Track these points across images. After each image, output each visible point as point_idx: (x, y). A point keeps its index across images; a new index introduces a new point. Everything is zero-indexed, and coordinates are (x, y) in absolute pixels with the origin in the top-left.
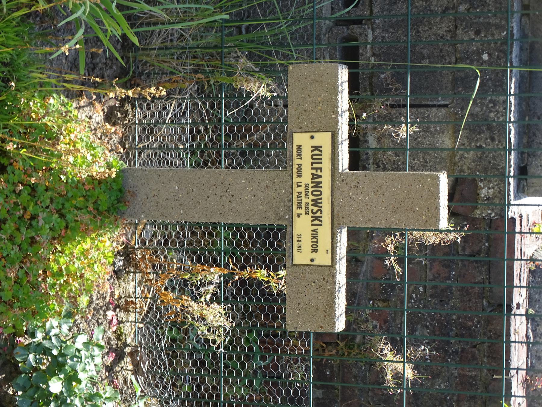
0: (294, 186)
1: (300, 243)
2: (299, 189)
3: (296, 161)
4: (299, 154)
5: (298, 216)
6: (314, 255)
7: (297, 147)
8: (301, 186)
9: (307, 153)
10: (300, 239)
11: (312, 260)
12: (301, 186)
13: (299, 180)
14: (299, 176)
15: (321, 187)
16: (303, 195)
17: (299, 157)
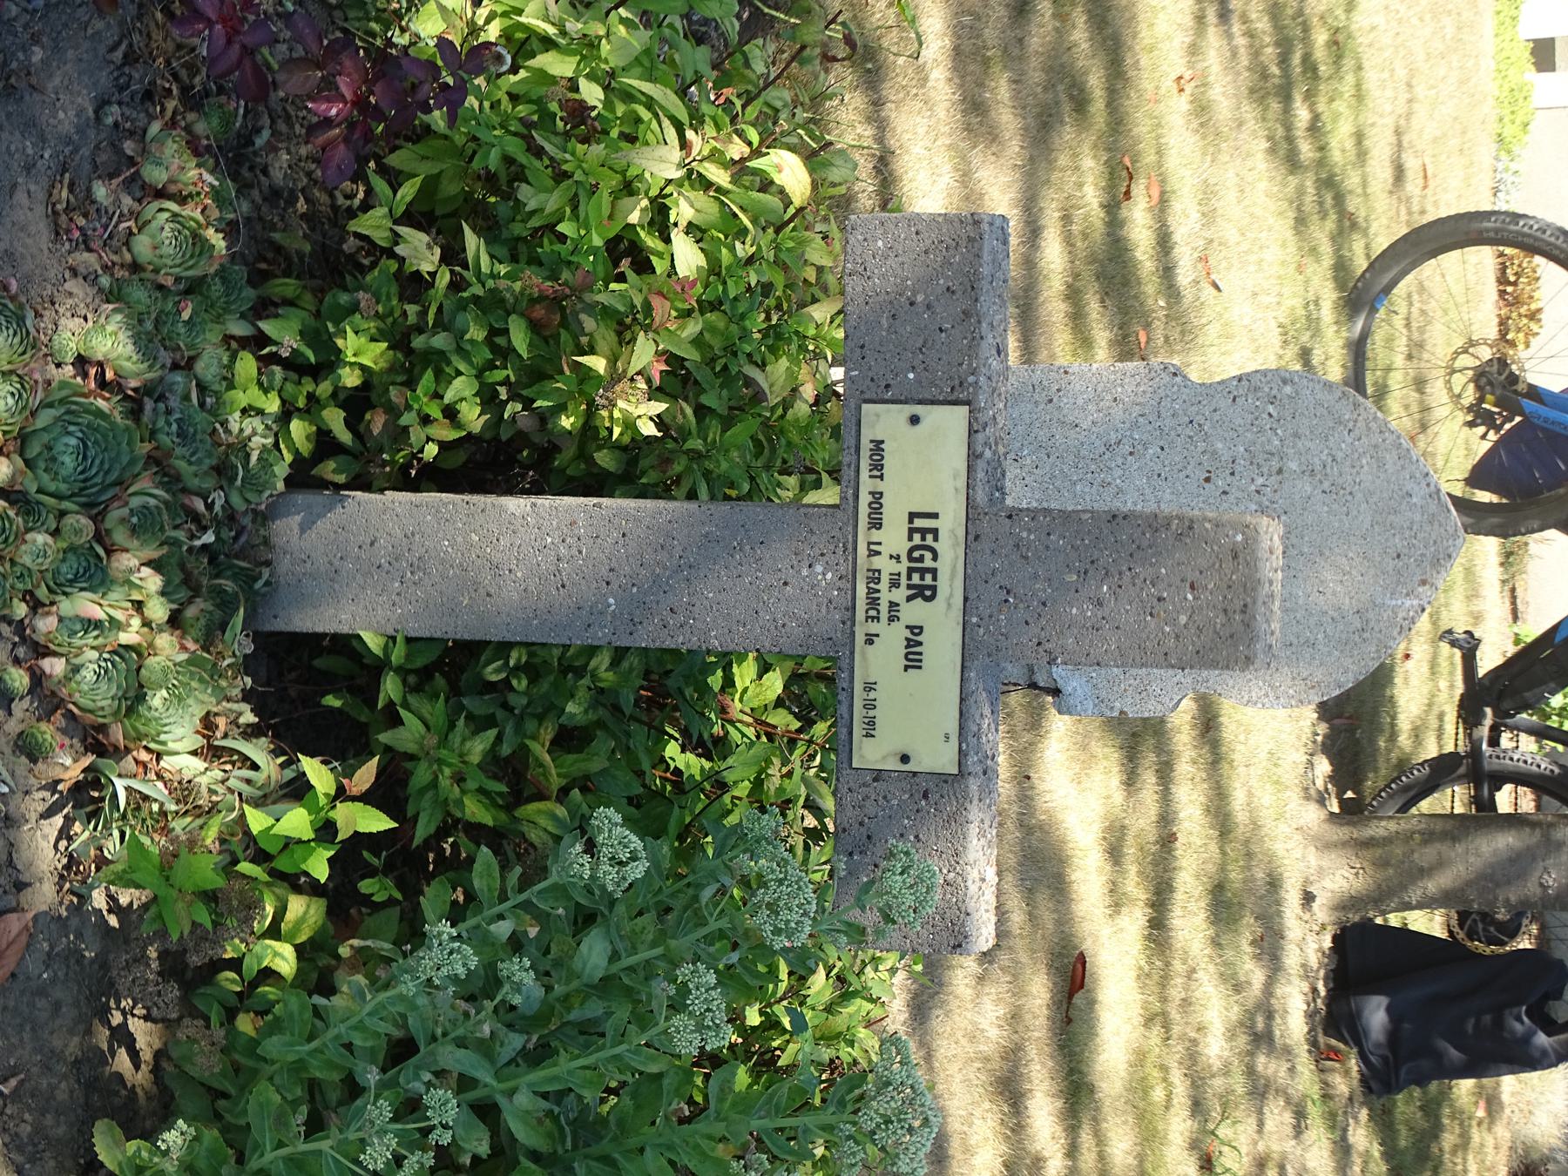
0: (862, 550)
1: (871, 713)
3: (867, 484)
4: (878, 467)
7: (871, 446)
8: (879, 553)
11: (905, 759)
12: (879, 553)
13: (876, 535)
14: (876, 524)
16: (885, 579)
17: (876, 473)
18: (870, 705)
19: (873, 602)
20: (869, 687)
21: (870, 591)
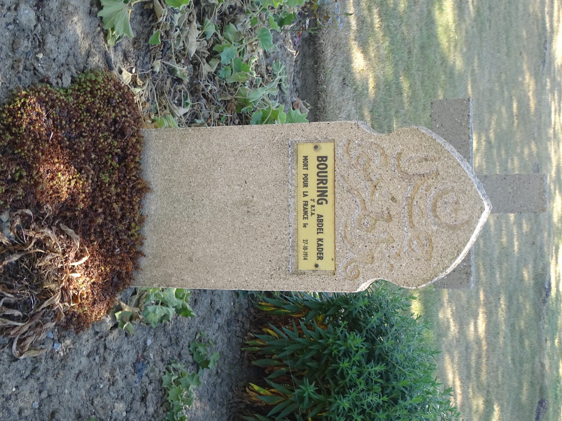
1: (306, 251)
2: (306, 199)
4: (306, 165)
5: (305, 225)
6: (319, 262)
9: (313, 163)
10: (306, 245)
12: (307, 195)
13: (305, 189)
14: (306, 185)
15: (327, 196)
17: (305, 167)
18: (305, 248)
19: (306, 213)
20: (306, 241)
21: (305, 209)
